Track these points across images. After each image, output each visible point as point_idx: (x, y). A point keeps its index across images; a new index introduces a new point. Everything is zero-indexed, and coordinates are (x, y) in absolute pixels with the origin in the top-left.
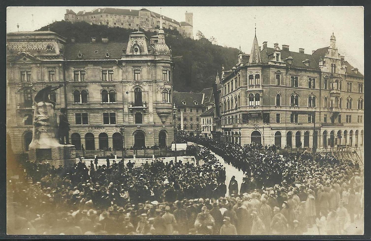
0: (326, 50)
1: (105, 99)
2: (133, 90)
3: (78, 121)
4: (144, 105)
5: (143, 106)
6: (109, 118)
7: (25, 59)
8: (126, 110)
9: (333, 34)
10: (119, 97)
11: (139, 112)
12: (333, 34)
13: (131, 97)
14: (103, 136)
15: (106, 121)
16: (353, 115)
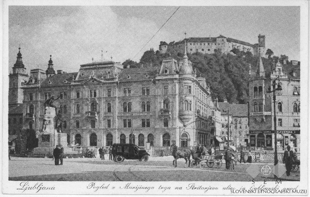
7: (93, 81)
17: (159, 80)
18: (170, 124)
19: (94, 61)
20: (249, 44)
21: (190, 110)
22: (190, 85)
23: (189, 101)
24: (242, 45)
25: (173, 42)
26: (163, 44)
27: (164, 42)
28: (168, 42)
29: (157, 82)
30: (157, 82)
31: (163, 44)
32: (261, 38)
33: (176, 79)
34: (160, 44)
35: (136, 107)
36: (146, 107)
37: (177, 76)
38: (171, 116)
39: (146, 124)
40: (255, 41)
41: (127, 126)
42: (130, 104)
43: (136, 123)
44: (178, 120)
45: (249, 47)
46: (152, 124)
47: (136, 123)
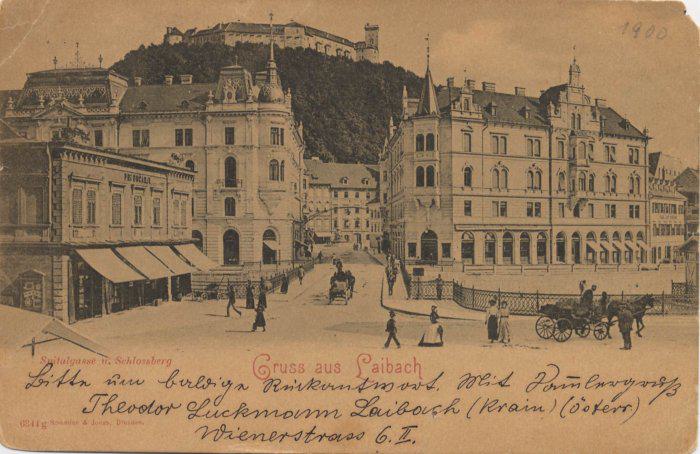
0: (564, 87)
4: (239, 185)
5: (235, 186)
16: (618, 204)
17: (213, 114)
18: (239, 211)
19: (60, 66)
20: (347, 43)
22: (280, 127)
24: (333, 44)
25: (194, 30)
28: (183, 32)
29: (209, 118)
30: (209, 118)
33: (252, 113)
34: (165, 33)
37: (255, 106)
38: (241, 193)
40: (359, 36)
45: (348, 48)
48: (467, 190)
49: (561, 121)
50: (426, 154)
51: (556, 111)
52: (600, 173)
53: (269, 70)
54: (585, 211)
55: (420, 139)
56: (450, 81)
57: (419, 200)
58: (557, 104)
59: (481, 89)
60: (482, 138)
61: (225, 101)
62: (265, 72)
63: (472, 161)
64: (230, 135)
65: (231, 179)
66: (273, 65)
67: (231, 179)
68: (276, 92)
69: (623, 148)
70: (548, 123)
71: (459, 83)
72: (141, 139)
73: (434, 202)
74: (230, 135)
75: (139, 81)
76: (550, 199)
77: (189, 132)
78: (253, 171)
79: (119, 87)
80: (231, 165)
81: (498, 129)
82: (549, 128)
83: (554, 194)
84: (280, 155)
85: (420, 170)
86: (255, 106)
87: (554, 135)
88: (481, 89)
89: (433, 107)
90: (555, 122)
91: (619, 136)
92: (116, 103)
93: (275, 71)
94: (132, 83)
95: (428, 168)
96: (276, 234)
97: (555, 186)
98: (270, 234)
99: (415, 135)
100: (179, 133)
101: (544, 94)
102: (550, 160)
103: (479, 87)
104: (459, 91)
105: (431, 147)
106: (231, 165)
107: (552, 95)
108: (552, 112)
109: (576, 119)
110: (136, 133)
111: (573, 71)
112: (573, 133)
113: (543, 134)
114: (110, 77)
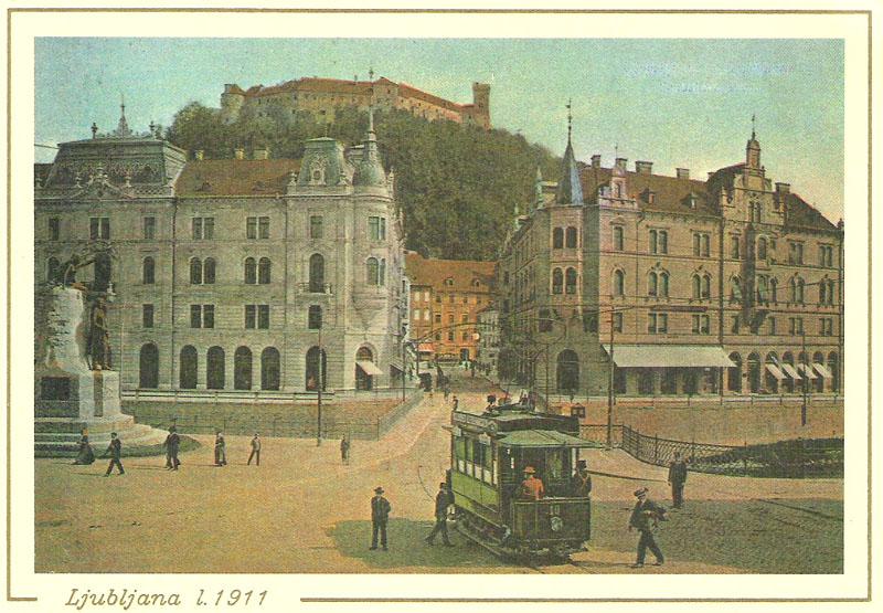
0: (739, 169)
1: (250, 278)
2: (307, 257)
3: (195, 323)
4: (328, 290)
6: (258, 317)
7: (101, 194)
8: (291, 299)
9: (754, 134)
10: (277, 273)
11: (317, 304)
12: (754, 134)
13: (303, 273)
14: (244, 353)
15: (250, 323)
16: (806, 317)
20: (451, 106)
21: (382, 284)
23: (380, 260)
25: (258, 88)
26: (232, 90)
27: (234, 87)
28: (245, 88)
29: (291, 203)
31: (232, 90)
32: (482, 92)
35: (232, 270)
36: (259, 272)
37: (349, 191)
39: (258, 317)
41: (202, 325)
42: (211, 266)
43: (231, 317)
44: (348, 308)
46: (275, 317)
47: (231, 317)
48: (618, 301)
49: (736, 210)
50: (565, 252)
51: (730, 198)
52: (783, 274)
53: (367, 143)
54: (765, 327)
55: (558, 232)
56: (596, 159)
57: (555, 311)
58: (730, 188)
59: (634, 170)
60: (639, 234)
61: (312, 182)
62: (362, 146)
63: (619, 259)
64: (316, 222)
65: (317, 284)
66: (372, 137)
67: (317, 284)
68: (378, 171)
69: (811, 243)
70: (720, 213)
71: (608, 163)
72: (205, 228)
73: (575, 312)
74: (316, 222)
75: (200, 156)
76: (721, 311)
77: (265, 222)
78: (346, 271)
79: (175, 163)
80: (317, 263)
81: (659, 224)
82: (721, 223)
83: (726, 304)
84: (382, 252)
85: (557, 272)
86: (349, 191)
87: (726, 230)
88: (634, 170)
89: (577, 194)
90: (728, 213)
91: (807, 231)
92: (172, 184)
93: (375, 146)
94: (192, 156)
95: (568, 271)
96: (374, 353)
97: (727, 292)
98: (366, 353)
99: (552, 229)
100: (251, 223)
101: (714, 177)
102: (721, 262)
103: (631, 167)
104: (609, 172)
105: (572, 244)
106: (317, 263)
107: (723, 178)
108: (725, 198)
109: (756, 208)
110: (197, 222)
111: (753, 147)
112: (750, 228)
113: (710, 227)
114: (165, 150)
